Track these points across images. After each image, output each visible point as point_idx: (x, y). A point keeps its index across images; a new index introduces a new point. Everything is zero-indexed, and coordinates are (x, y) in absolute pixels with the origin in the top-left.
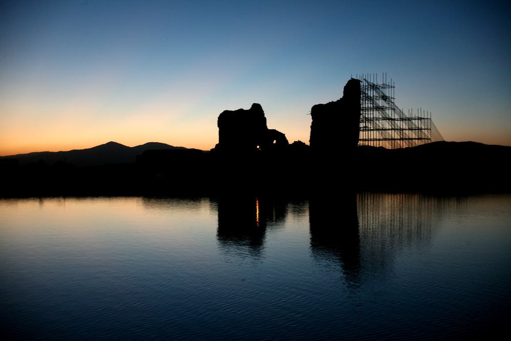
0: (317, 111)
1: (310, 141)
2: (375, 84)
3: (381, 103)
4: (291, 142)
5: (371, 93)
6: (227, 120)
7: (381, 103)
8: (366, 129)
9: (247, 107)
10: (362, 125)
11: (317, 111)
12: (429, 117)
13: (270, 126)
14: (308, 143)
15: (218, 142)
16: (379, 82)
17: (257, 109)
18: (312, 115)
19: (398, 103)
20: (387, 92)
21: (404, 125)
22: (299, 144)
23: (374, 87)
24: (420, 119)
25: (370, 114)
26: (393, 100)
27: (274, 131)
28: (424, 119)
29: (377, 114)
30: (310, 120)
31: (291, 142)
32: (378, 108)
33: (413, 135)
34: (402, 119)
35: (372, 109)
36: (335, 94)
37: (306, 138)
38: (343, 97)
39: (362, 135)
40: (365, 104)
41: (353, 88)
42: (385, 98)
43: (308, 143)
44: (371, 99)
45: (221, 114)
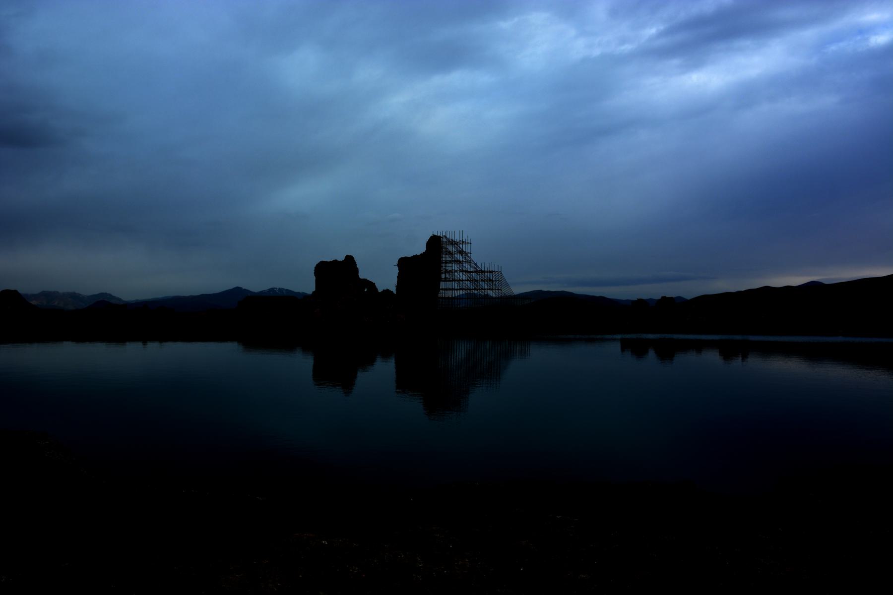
0: (404, 263)
1: (398, 287)
2: (454, 239)
3: (459, 257)
4: (380, 290)
5: (450, 248)
6: (324, 270)
7: (459, 257)
8: (446, 280)
9: (341, 258)
10: (443, 276)
11: (404, 263)
12: (500, 270)
13: (362, 275)
14: (395, 292)
15: (314, 290)
16: (457, 238)
17: (350, 259)
18: (398, 267)
19: (474, 257)
20: (465, 248)
21: (475, 276)
22: (387, 292)
23: (452, 243)
24: (492, 272)
25: (449, 267)
26: (469, 255)
27: (365, 281)
28: (495, 272)
29: (455, 267)
30: (396, 271)
31: (380, 290)
32: (457, 262)
33: (470, 285)
34: (476, 272)
35: (451, 262)
36: (420, 248)
37: (393, 289)
38: (426, 251)
39: (443, 285)
40: (446, 258)
41: (435, 243)
42: (462, 252)
43: (395, 292)
44: (450, 253)
45: (317, 265)
